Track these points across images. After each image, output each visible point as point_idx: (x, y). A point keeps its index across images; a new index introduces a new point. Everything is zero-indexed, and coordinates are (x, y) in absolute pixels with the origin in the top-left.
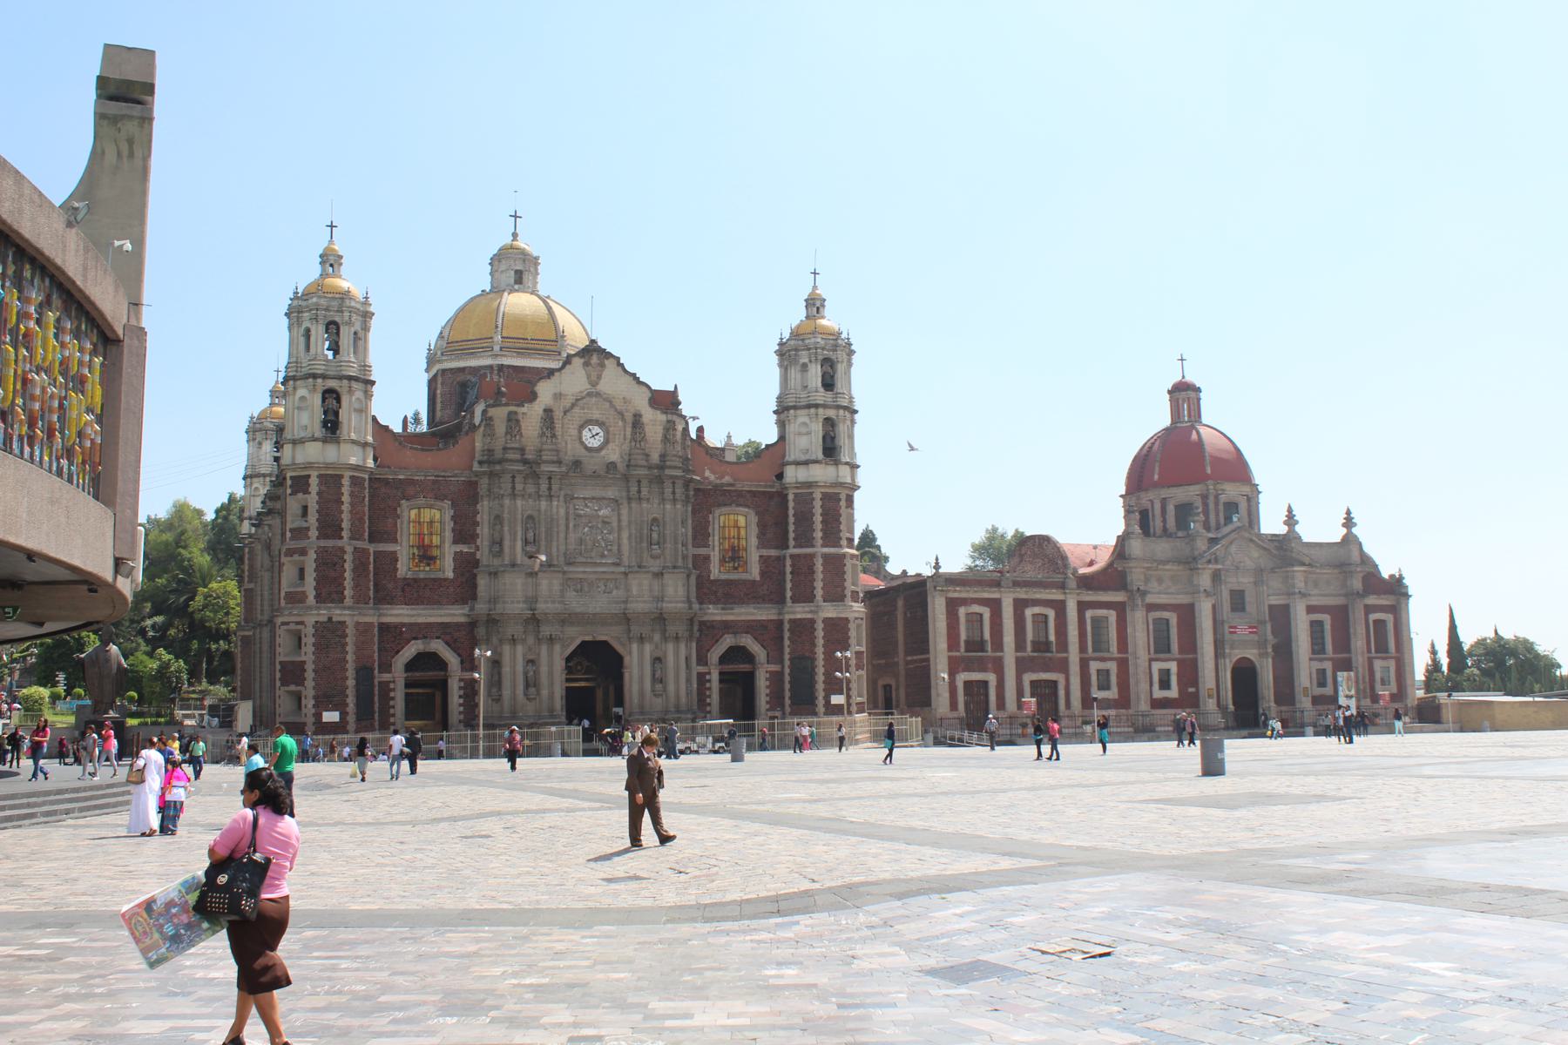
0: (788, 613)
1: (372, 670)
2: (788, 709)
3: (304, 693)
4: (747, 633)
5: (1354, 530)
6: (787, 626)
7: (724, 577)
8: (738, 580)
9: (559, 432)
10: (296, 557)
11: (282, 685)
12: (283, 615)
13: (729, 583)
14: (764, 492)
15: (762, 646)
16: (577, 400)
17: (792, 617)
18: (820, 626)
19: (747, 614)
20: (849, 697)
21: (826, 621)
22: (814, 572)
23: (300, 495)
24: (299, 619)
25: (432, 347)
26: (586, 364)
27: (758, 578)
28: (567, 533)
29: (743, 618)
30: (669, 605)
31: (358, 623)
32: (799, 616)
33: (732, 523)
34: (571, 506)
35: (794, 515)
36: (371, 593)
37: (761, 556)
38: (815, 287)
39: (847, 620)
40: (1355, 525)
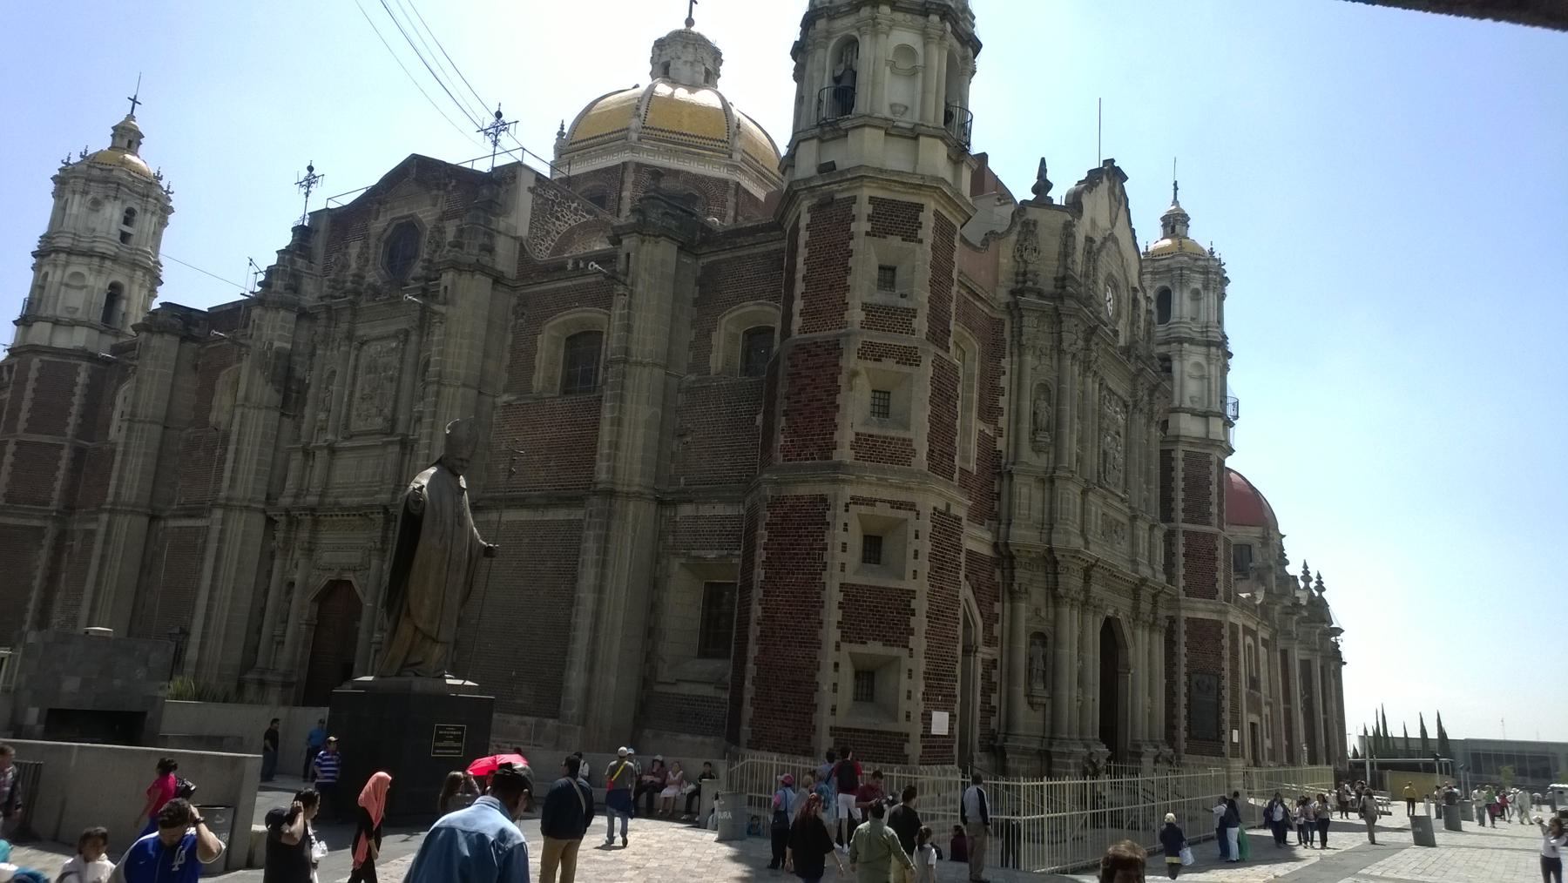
0: (1187, 609)
2: (1184, 745)
3: (907, 663)
5: (1324, 594)
6: (1183, 627)
10: (889, 364)
11: (846, 637)
12: (860, 481)
17: (1191, 615)
18: (1226, 632)
22: (1215, 559)
23: (895, 241)
24: (902, 496)
25: (566, 130)
32: (1200, 615)
35: (1184, 479)
38: (1175, 202)
40: (1324, 589)
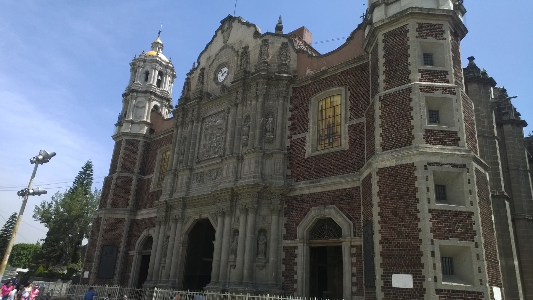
1: (118, 247)
4: (332, 203)
7: (315, 154)
8: (329, 154)
9: (205, 81)
13: (320, 158)
14: (356, 67)
15: (348, 216)
16: (216, 56)
19: (332, 184)
20: (419, 279)
21: (381, 172)
26: (222, 32)
27: (347, 148)
28: (200, 142)
29: (329, 188)
30: (246, 180)
31: (109, 218)
33: (328, 105)
34: (204, 124)
36: (130, 202)
37: (350, 126)
39: (412, 167)
